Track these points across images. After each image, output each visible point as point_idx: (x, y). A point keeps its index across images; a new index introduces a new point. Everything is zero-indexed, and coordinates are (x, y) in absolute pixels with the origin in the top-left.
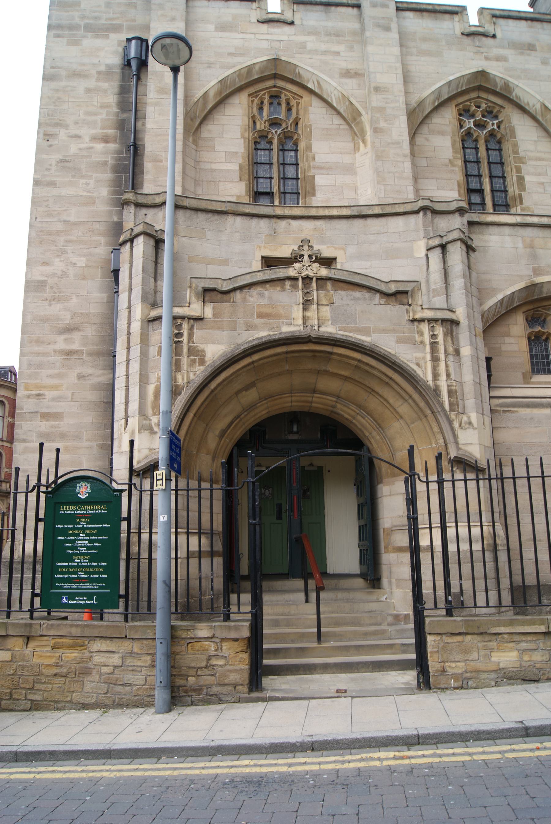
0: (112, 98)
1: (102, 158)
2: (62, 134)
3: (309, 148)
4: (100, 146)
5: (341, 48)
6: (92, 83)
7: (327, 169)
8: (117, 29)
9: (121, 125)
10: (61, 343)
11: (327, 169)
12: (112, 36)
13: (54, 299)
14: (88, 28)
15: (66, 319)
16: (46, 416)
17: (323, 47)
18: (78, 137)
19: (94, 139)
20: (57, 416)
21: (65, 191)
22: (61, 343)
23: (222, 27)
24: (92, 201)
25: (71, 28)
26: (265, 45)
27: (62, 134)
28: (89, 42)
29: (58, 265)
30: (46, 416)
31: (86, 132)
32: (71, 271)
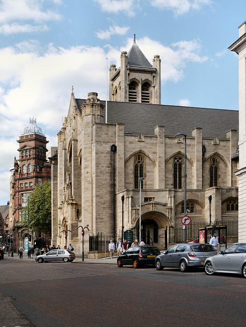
0: (109, 158)
1: (107, 171)
2: (100, 166)
3: (145, 168)
4: (107, 168)
5: (153, 147)
6: (105, 155)
7: (148, 172)
8: (109, 142)
9: (111, 164)
10: (102, 206)
11: (148, 172)
12: (109, 144)
13: (101, 198)
14: (104, 142)
15: (103, 202)
16: (101, 219)
17: (150, 147)
18: (103, 166)
19: (106, 167)
20: (103, 218)
21: (102, 178)
22: (102, 206)
23: (131, 143)
24: (106, 180)
25: (101, 142)
26: (139, 147)
27: (100, 166)
28: (104, 145)
29: (101, 192)
30: (101, 219)
31: (105, 166)
32: (104, 193)
